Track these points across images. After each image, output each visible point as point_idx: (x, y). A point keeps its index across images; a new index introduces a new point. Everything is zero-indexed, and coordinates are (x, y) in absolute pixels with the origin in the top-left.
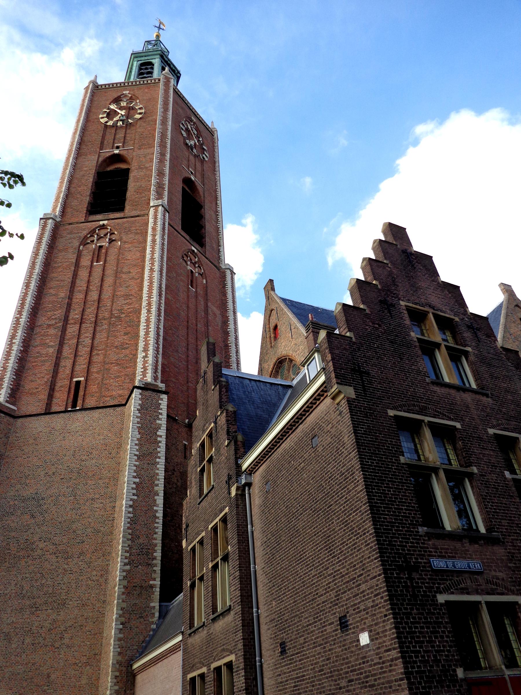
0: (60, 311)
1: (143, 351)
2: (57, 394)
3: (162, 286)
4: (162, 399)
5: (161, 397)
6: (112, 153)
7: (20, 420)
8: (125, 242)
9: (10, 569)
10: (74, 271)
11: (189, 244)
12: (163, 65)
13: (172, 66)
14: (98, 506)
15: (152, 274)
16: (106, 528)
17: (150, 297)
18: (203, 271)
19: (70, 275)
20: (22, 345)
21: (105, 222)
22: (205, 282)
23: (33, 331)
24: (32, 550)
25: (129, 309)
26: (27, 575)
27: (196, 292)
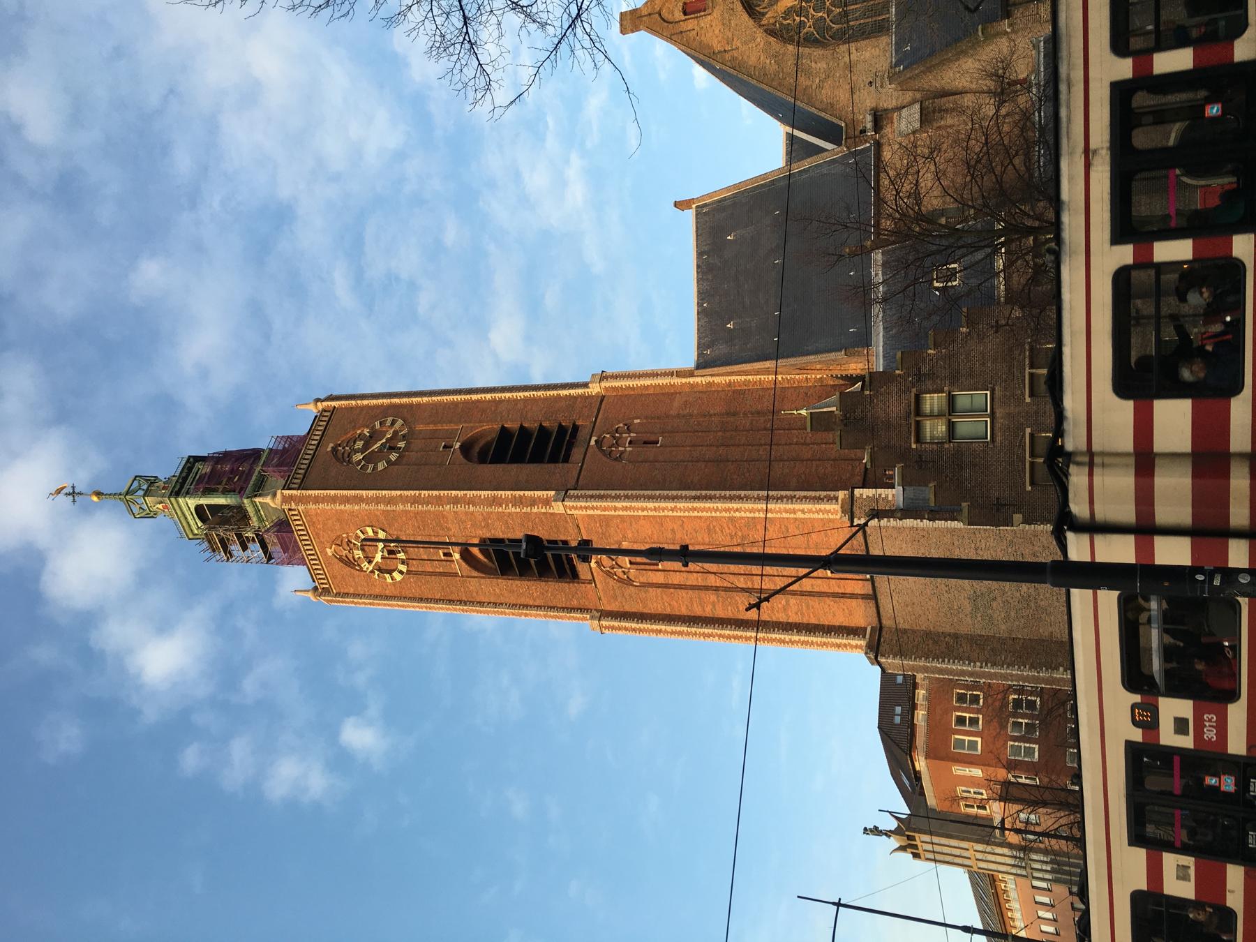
0: (737, 598)
1: (795, 514)
2: (848, 591)
3: (693, 495)
4: (861, 495)
5: (858, 496)
6: (461, 561)
7: (884, 622)
8: (624, 536)
9: (1048, 612)
10: (675, 588)
11: (590, 450)
13: (184, 474)
14: (984, 544)
16: (1007, 535)
17: (717, 510)
18: (621, 425)
19: (683, 593)
20: (790, 632)
22: (639, 421)
23: (768, 621)
24: (1029, 596)
25: (729, 528)
26: (1055, 598)
27: (662, 433)
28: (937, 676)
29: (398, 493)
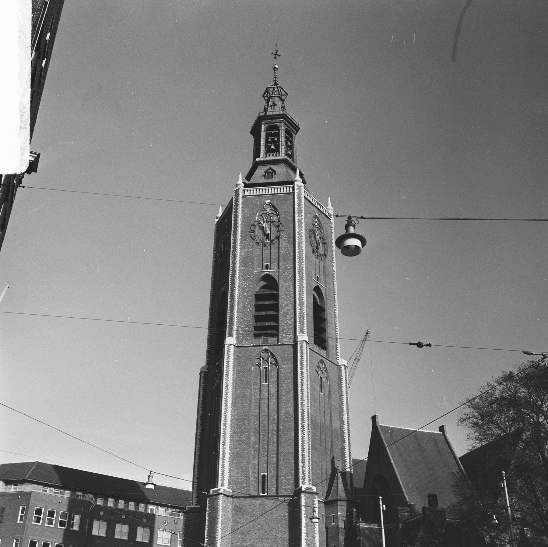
5: (315, 496)
6: (264, 274)
12: (287, 127)
15: (302, 403)
21: (267, 348)
28: (207, 524)
29: (304, 250)
